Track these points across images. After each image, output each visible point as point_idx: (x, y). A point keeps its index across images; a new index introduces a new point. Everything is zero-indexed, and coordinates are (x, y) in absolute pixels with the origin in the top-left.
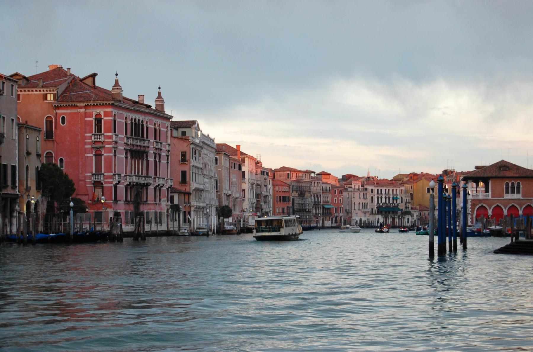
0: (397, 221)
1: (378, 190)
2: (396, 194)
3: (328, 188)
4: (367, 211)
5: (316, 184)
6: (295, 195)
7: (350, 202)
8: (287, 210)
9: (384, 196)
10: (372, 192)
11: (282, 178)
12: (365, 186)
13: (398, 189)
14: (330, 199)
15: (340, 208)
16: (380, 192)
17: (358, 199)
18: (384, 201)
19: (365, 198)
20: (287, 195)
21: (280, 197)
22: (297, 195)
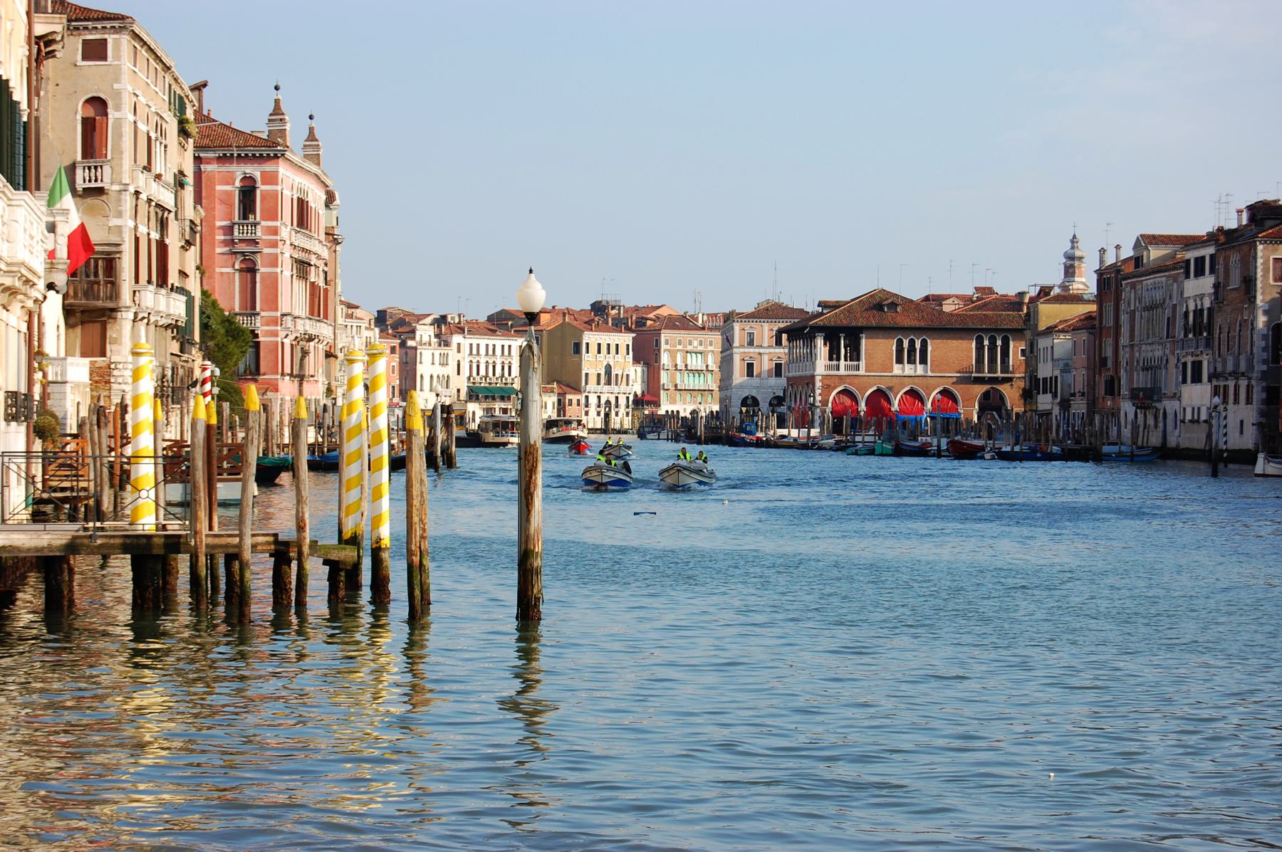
9: (483, 361)
10: (459, 351)
12: (444, 338)
16: (475, 352)
17: (426, 367)
18: (482, 372)
19: (444, 364)
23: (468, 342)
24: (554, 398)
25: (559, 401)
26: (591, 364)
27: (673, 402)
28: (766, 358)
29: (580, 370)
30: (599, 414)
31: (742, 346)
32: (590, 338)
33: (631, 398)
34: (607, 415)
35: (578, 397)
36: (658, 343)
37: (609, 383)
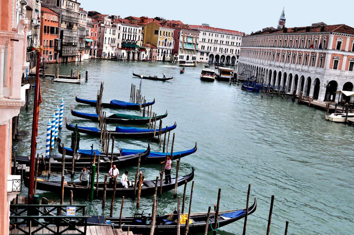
0: (136, 56)
1: (124, 28)
2: (136, 33)
3: (89, 22)
4: (115, 46)
5: (83, 16)
6: (64, 26)
7: (102, 36)
8: (55, 43)
9: (127, 34)
10: (119, 30)
11: (50, 4)
13: (138, 29)
14: (90, 33)
15: (95, 42)
17: (108, 35)
18: (127, 38)
19: (114, 34)
20: (56, 26)
21: (48, 27)
22: (66, 27)
23: (123, 26)
24: (149, 50)
25: (151, 50)
26: (160, 39)
27: (182, 52)
28: (345, 59)
29: (157, 40)
30: (162, 56)
31: (333, 49)
32: (161, 29)
33: (171, 50)
34: (164, 56)
35: (156, 49)
36: (179, 33)
37: (165, 45)
